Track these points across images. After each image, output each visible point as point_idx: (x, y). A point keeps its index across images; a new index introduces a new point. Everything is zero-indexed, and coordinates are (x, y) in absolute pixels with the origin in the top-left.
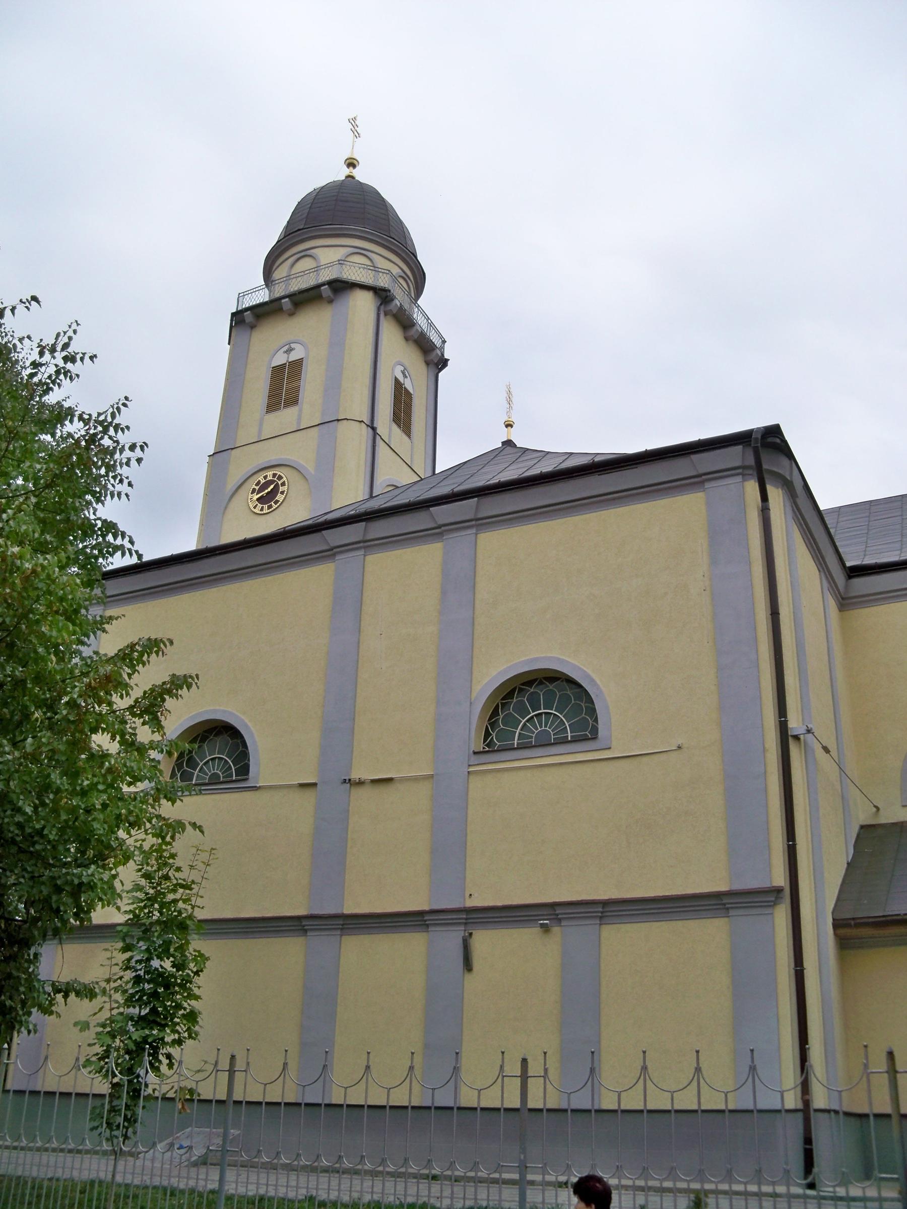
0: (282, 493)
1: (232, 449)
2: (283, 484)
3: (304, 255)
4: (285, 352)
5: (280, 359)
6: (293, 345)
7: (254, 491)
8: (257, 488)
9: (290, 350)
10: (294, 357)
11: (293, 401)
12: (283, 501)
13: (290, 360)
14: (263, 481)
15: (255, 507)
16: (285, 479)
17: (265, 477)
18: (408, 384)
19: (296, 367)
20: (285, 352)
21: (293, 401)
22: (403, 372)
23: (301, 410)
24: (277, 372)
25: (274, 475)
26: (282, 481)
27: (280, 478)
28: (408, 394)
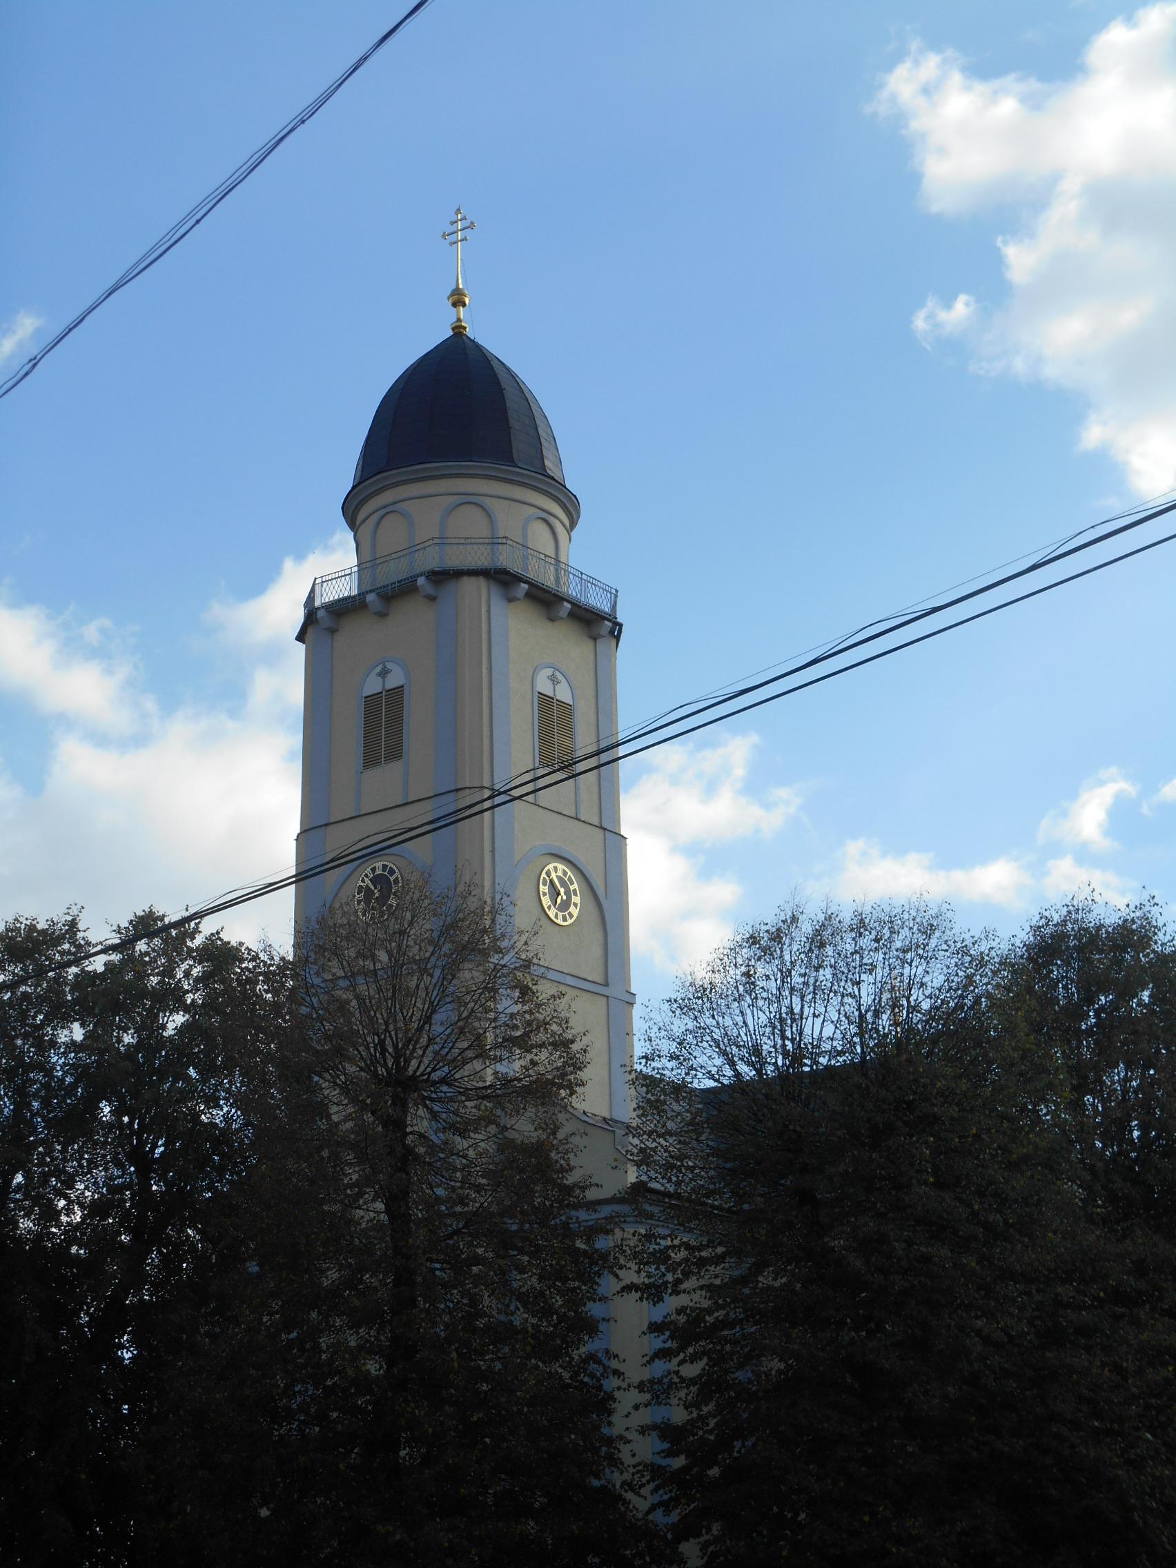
1: (326, 825)
3: (388, 510)
4: (379, 675)
5: (373, 685)
6: (389, 665)
9: (384, 673)
10: (392, 682)
11: (395, 753)
13: (388, 687)
16: (397, 874)
17: (374, 870)
20: (379, 675)
21: (395, 753)
24: (372, 703)
25: (385, 867)
26: (395, 876)
27: (392, 872)
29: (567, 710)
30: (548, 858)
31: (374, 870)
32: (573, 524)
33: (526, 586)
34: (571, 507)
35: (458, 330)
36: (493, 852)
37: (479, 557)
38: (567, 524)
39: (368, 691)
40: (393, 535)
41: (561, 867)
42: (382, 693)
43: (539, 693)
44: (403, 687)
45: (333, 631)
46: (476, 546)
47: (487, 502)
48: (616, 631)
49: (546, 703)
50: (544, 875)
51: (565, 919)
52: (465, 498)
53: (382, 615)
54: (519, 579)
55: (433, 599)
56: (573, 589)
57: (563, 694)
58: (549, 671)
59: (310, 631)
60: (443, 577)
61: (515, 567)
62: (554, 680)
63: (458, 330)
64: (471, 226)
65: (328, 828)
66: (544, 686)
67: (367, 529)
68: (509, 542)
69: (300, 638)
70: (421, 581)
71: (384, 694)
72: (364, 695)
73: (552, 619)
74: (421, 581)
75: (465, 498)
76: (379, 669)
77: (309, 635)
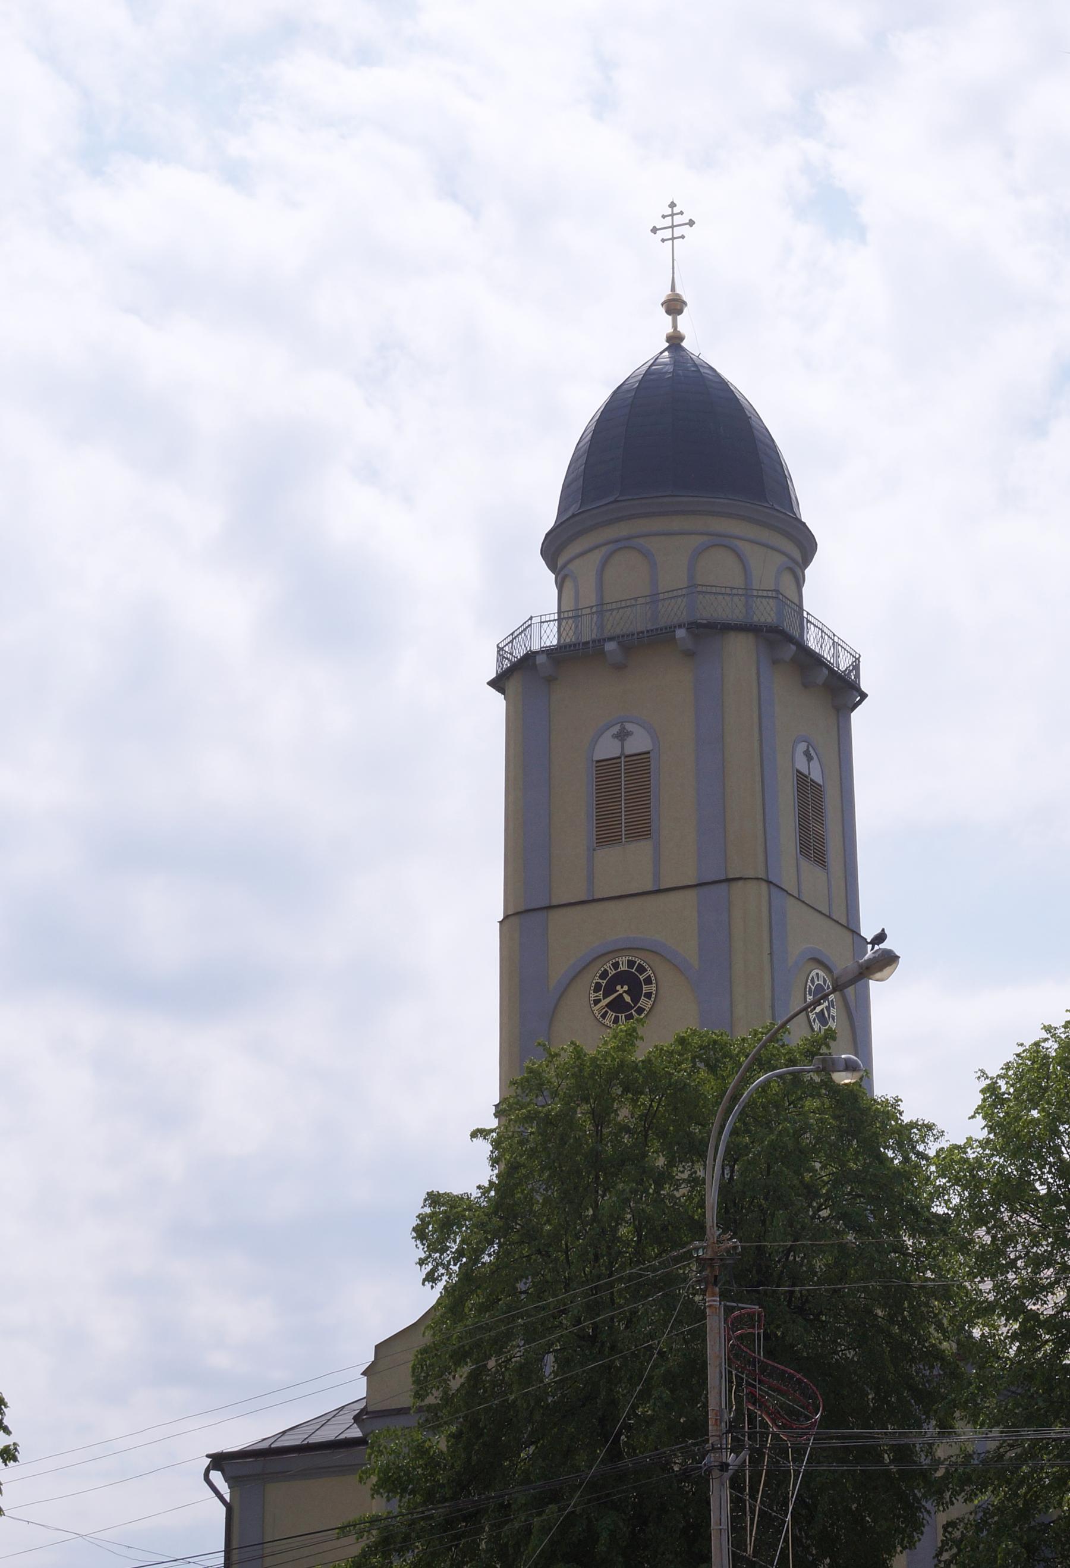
0: (648, 996)
2: (648, 981)
4: (615, 736)
5: (608, 748)
6: (629, 727)
7: (598, 987)
8: (604, 982)
9: (623, 735)
12: (651, 1009)
13: (628, 751)
15: (604, 1016)
18: (816, 776)
19: (640, 763)
20: (615, 736)
22: (807, 754)
25: (631, 964)
27: (641, 969)
28: (817, 788)
35: (675, 341)
39: (600, 755)
42: (619, 758)
43: (798, 771)
44: (649, 753)
45: (550, 680)
46: (720, 597)
47: (745, 548)
49: (803, 781)
50: (809, 983)
55: (690, 654)
63: (675, 341)
66: (801, 764)
68: (781, 597)
69: (497, 683)
70: (681, 633)
71: (622, 758)
72: (595, 759)
73: (806, 686)
74: (681, 633)
76: (616, 729)
77: (512, 685)
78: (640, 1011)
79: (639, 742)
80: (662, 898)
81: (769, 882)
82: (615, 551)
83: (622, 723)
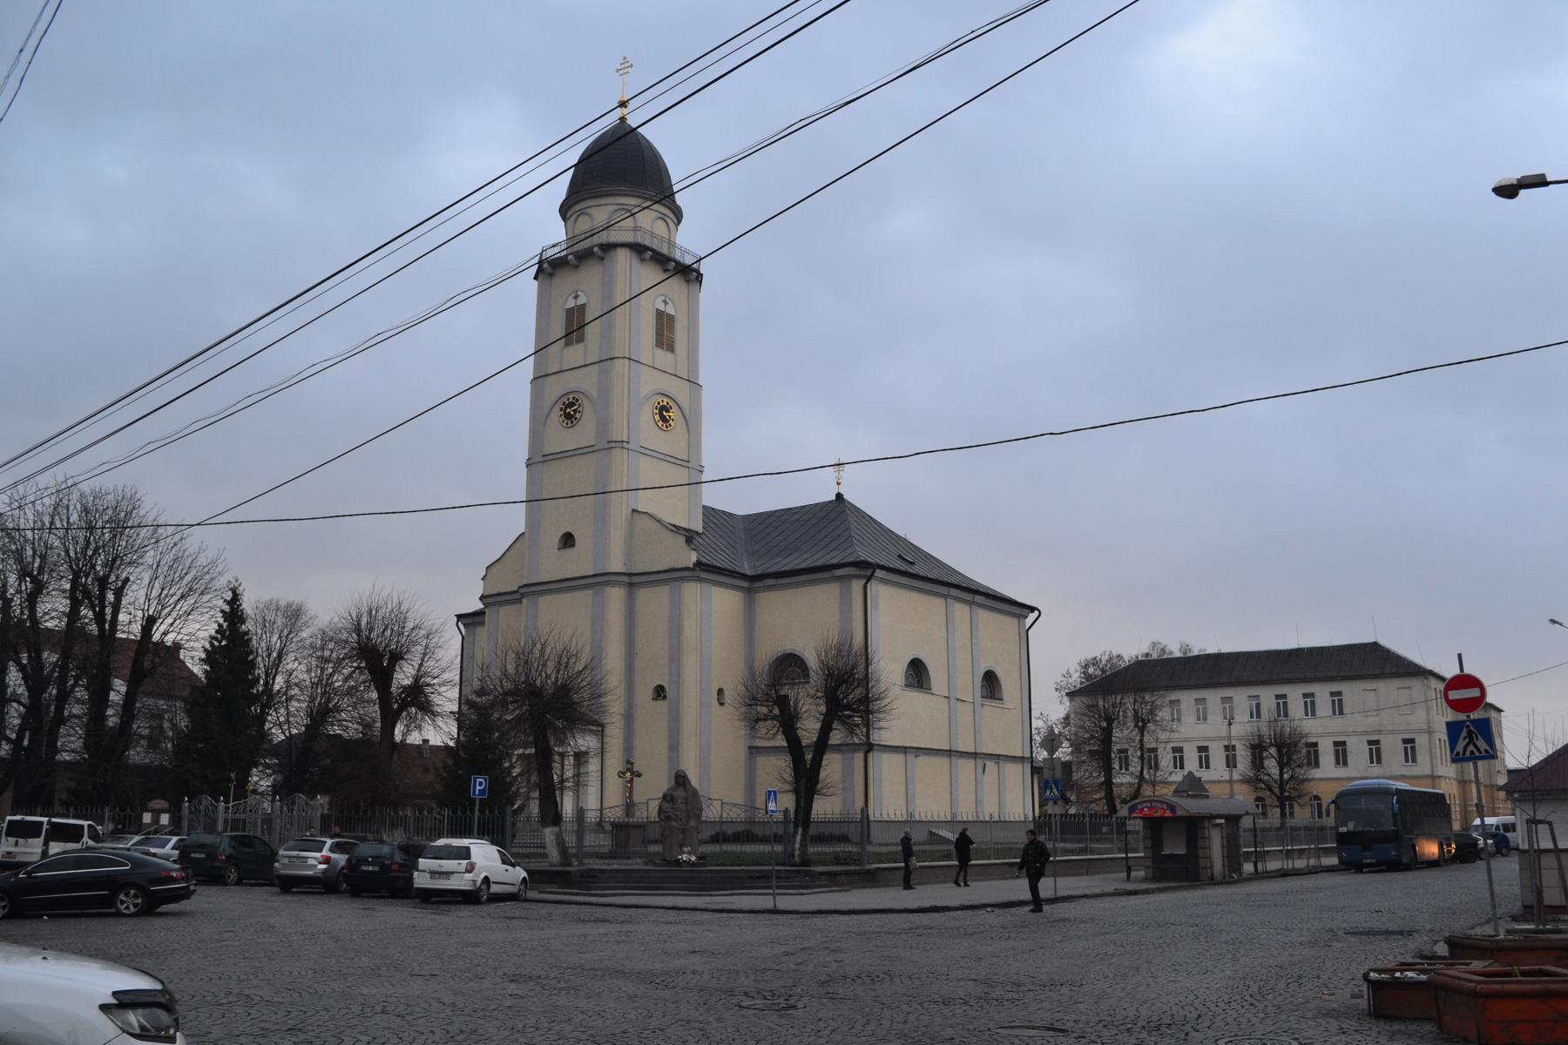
1: (545, 376)
3: (582, 213)
5: (571, 304)
6: (579, 293)
9: (576, 297)
13: (578, 304)
14: (567, 402)
17: (568, 399)
23: (586, 346)
25: (574, 398)
29: (671, 318)
30: (660, 396)
31: (568, 399)
32: (679, 221)
33: (650, 253)
34: (678, 215)
36: (629, 391)
37: (628, 237)
38: (676, 221)
39: (567, 307)
40: (584, 225)
41: (665, 400)
45: (551, 275)
48: (699, 278)
51: (667, 427)
52: (621, 207)
53: (577, 267)
54: (646, 248)
56: (678, 256)
57: (670, 310)
58: (663, 298)
59: (540, 275)
60: (609, 248)
61: (647, 243)
62: (665, 302)
64: (632, 66)
65: (547, 378)
66: (661, 307)
67: (570, 222)
69: (536, 278)
70: (596, 249)
74: (596, 249)
75: (621, 207)
76: (573, 295)
77: (539, 278)
78: (576, 419)
79: (581, 301)
80: (586, 368)
81: (629, 359)
82: (578, 216)
83: (576, 291)
